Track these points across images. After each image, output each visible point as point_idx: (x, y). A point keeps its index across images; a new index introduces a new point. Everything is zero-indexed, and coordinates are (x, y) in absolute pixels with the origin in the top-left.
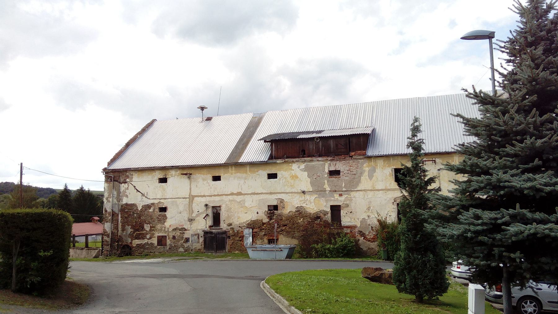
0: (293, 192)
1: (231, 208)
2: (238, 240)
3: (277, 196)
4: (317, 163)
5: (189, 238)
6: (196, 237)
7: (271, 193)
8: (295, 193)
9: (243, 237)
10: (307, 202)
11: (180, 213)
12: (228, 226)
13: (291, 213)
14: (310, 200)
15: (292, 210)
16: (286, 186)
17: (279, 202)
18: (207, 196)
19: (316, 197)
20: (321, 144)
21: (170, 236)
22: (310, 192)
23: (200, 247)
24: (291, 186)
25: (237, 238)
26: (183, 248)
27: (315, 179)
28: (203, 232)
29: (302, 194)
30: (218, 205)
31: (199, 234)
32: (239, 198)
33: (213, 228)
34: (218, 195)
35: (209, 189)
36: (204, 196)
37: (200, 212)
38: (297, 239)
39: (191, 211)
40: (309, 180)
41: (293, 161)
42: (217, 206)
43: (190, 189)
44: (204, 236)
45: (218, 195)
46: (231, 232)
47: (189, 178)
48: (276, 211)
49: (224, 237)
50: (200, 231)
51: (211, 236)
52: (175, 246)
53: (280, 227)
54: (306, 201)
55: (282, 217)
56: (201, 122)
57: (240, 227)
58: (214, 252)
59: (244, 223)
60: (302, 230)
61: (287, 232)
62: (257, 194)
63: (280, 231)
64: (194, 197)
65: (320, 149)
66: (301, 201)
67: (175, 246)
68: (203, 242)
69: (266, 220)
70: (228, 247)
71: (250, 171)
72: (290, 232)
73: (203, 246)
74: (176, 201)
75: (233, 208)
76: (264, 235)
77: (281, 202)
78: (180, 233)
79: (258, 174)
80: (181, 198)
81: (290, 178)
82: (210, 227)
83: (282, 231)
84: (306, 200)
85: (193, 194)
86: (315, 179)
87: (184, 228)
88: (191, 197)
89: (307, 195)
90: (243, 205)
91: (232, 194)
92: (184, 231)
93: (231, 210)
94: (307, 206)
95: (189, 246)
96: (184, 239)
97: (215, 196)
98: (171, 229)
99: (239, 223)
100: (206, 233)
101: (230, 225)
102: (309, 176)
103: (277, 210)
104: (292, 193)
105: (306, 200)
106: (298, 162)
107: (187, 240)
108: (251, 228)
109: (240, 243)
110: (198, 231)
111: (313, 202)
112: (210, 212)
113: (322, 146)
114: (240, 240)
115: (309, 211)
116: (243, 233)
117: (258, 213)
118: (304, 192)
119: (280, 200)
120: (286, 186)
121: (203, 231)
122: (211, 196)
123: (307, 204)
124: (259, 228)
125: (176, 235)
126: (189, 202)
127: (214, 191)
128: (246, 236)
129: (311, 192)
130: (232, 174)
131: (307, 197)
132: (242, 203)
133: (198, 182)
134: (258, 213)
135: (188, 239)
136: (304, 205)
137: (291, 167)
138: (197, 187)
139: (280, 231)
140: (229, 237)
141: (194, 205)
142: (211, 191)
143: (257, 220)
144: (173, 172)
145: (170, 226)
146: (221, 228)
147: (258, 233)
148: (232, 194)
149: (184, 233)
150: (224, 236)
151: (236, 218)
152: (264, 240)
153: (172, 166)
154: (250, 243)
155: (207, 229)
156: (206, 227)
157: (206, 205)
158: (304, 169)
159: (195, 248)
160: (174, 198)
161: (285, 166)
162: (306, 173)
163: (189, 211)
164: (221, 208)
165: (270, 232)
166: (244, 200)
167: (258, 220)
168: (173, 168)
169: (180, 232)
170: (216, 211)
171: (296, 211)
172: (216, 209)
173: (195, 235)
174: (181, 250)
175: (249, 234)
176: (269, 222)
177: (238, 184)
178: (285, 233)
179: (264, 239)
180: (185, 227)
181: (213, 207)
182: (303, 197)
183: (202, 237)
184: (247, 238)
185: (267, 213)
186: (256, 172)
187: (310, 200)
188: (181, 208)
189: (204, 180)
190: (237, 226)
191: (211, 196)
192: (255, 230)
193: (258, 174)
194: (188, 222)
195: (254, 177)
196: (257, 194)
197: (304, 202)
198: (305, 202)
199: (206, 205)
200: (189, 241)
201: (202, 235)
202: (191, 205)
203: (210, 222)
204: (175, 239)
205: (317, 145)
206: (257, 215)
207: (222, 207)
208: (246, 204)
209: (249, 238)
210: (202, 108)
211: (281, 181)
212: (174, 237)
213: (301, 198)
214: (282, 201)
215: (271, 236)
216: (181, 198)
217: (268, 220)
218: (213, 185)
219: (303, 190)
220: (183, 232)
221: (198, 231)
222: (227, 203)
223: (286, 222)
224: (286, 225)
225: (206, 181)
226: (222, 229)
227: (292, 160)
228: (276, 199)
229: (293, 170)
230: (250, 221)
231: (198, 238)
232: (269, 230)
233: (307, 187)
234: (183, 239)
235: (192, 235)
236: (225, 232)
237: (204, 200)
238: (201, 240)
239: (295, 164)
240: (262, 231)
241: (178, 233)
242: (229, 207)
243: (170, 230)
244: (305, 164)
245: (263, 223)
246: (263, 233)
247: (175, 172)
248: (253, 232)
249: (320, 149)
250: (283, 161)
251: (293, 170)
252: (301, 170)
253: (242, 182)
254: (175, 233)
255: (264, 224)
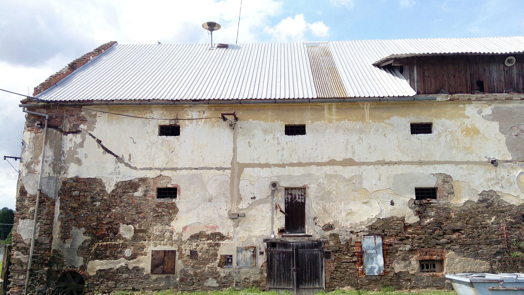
0: (471, 161)
1: (330, 193)
2: (350, 262)
3: (435, 169)
4: (518, 105)
5: (231, 256)
6: (249, 254)
7: (421, 163)
8: (475, 163)
9: (361, 255)
10: (503, 182)
11: (210, 200)
12: (324, 230)
13: (469, 205)
14: (510, 178)
15: (472, 199)
16: (454, 149)
17: (440, 182)
18: (275, 165)
19: (521, 173)
20: (515, 71)
21: (183, 252)
22: (507, 161)
23: (258, 278)
24: (466, 149)
25: (347, 257)
26: (216, 278)
27: (517, 136)
28: (265, 244)
29: (489, 165)
30: (301, 185)
31: (255, 248)
32: (348, 172)
33: (287, 234)
34: (300, 164)
35: (278, 151)
36: (267, 165)
37: (256, 199)
38: (487, 260)
39: (236, 196)
40: (503, 138)
41: (469, 100)
42: (296, 188)
43: (235, 150)
44: (267, 251)
45: (300, 164)
46: (332, 243)
47: (232, 126)
48: (434, 201)
49: (316, 256)
50: (257, 240)
51: (284, 253)
52: (196, 274)
53: (444, 234)
54: (501, 180)
55: (449, 213)
56: (210, 49)
57: (352, 232)
58: (291, 287)
59: (362, 223)
60: (495, 241)
61: (463, 245)
62: (390, 163)
63: (447, 243)
64: (242, 167)
65: (515, 81)
66: (489, 180)
67: (196, 274)
68: (265, 265)
69: (413, 219)
70: (324, 276)
71: (371, 117)
72: (469, 245)
73: (266, 275)
74: (201, 174)
75: (334, 193)
76: (411, 251)
77: (445, 182)
78: (210, 245)
79: (390, 124)
80: (212, 169)
81: (462, 132)
82: (281, 231)
83: (452, 242)
84: (499, 177)
85: (240, 159)
86: (517, 136)
87: (219, 234)
88: (236, 168)
89: (501, 168)
90: (357, 186)
91: (332, 163)
92: (219, 240)
93: (332, 196)
94: (504, 191)
95: (230, 274)
96: (219, 257)
97: (292, 165)
98: (186, 236)
99: (351, 224)
100: (272, 244)
101: (329, 227)
102: (502, 130)
103: (435, 198)
104: (468, 163)
105: (499, 177)
106: (480, 100)
107: (227, 260)
108: (379, 235)
109: (352, 267)
110: (254, 240)
111: (516, 183)
112: (281, 199)
113: (519, 75)
114: (353, 262)
115: (508, 201)
116: (361, 246)
117: (392, 203)
118: (494, 162)
119: (441, 178)
120: (454, 149)
121: (265, 240)
122: (283, 166)
123: (502, 187)
124: (397, 235)
125: (198, 249)
126: (232, 178)
127: (291, 156)
128: (369, 251)
129: (510, 161)
130: (330, 121)
131: (502, 171)
132: (354, 181)
133: (253, 135)
134: (392, 203)
135: (228, 259)
136: (497, 188)
137: (462, 112)
138: (250, 146)
139: (447, 243)
140: (327, 255)
141: (243, 183)
142: (283, 155)
143: (392, 217)
144: (194, 113)
145: (185, 228)
146: (307, 233)
147: (396, 246)
148: (332, 163)
149: (218, 245)
150: (316, 251)
151: (344, 214)
152: (410, 263)
153: (195, 100)
154: (379, 268)
155: (275, 236)
156: (273, 233)
157: (274, 185)
158: (490, 115)
159: (245, 278)
160: (196, 167)
161: (450, 109)
162: (496, 125)
163: (232, 196)
164: (308, 191)
165: (423, 245)
166: (360, 178)
167: (395, 219)
168: (195, 102)
169: (209, 241)
170: (291, 198)
171: (479, 200)
172: (291, 194)
173: (247, 249)
174: (212, 282)
175: (376, 248)
176: (419, 223)
177: (345, 142)
178: (457, 247)
179: (412, 259)
180: (221, 232)
181: (287, 189)
182: (493, 172)
183: (262, 253)
184: (371, 257)
185: (415, 203)
186: (385, 119)
187: (510, 178)
188: (212, 190)
189: (265, 131)
190: (346, 231)
191: (283, 166)
192: (387, 240)
193: (390, 124)
194: (229, 220)
195: (380, 130)
196: (390, 163)
197: (495, 181)
198: (498, 183)
199: (274, 185)
200: (231, 263)
201: (263, 250)
202: (236, 182)
203: (280, 222)
204: (196, 259)
205: (507, 73)
206: (390, 207)
207: (310, 190)
208: (366, 184)
209: (376, 256)
210: (212, 26)
211: (443, 139)
212: (193, 254)
213: (488, 174)
214: (446, 179)
215: (426, 254)
216: (212, 169)
217: (415, 219)
218: (287, 143)
219: (492, 157)
220: (217, 242)
221: (254, 240)
222: (321, 180)
223: (459, 224)
224: (458, 231)
225: (271, 135)
226: (311, 236)
227: (468, 97)
228: (434, 175)
229: (468, 117)
230: (375, 220)
231: (254, 256)
232: (421, 241)
233: (500, 151)
234: (216, 259)
235: (239, 250)
236: (318, 244)
237: (272, 174)
238: (262, 260)
239: (471, 105)
240: (406, 242)
241: (204, 245)
242: (326, 190)
243: (184, 239)
244: (493, 106)
245: (405, 224)
246: (408, 247)
247: (198, 113)
248: (383, 244)
249: (515, 81)
250: (449, 98)
251: (468, 117)
252: (485, 118)
253: (354, 138)
254: (197, 245)
255: (407, 227)
